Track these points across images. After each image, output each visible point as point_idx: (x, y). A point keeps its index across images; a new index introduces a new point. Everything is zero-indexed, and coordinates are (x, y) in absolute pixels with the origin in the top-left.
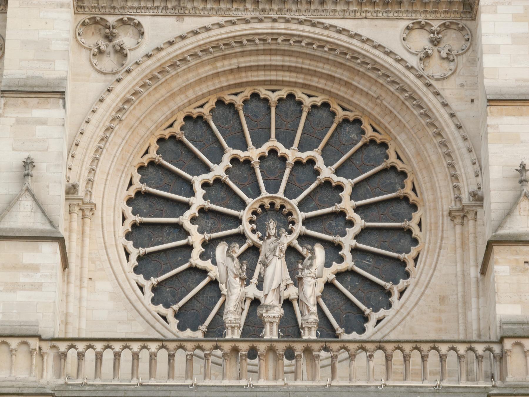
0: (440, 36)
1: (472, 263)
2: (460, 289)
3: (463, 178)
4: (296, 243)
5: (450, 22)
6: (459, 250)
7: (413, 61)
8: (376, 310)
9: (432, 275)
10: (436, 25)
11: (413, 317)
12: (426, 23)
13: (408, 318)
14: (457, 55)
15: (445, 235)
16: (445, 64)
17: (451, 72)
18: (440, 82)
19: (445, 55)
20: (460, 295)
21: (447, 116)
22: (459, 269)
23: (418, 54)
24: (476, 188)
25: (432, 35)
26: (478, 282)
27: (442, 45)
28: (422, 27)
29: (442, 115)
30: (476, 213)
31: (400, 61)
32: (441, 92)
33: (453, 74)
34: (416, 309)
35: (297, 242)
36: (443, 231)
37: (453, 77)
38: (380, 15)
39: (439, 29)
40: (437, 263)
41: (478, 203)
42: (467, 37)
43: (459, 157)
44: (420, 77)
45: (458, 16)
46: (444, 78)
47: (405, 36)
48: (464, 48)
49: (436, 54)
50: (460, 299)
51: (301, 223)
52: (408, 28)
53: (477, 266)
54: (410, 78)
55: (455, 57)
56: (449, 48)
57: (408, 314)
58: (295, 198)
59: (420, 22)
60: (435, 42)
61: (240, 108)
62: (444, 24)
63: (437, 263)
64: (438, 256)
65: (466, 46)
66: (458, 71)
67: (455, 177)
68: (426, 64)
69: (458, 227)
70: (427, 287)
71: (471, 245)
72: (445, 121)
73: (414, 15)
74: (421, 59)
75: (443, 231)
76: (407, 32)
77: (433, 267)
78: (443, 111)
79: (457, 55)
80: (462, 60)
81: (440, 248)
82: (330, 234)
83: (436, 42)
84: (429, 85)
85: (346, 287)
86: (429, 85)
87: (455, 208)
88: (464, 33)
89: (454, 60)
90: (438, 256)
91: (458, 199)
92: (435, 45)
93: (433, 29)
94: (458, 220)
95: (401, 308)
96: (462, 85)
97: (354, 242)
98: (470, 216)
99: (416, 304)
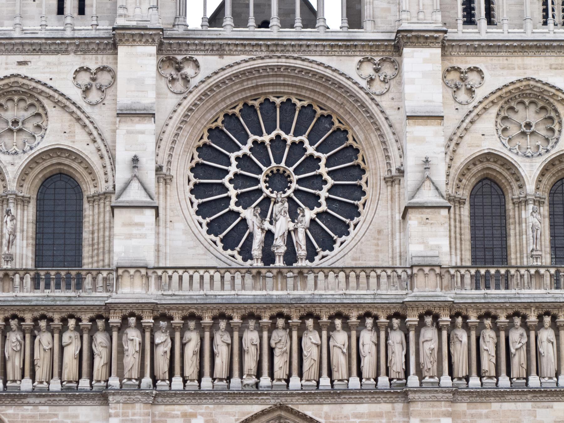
1: (397, 211)
2: (390, 226)
3: (392, 157)
4: (292, 195)
6: (390, 202)
7: (363, 84)
8: (340, 236)
10: (377, 59)
11: (362, 243)
12: (372, 58)
13: (359, 243)
15: (381, 192)
16: (383, 84)
17: (386, 90)
18: (379, 97)
19: (382, 79)
20: (390, 230)
21: (383, 119)
22: (389, 214)
24: (400, 165)
25: (375, 66)
27: (381, 72)
28: (369, 61)
29: (380, 118)
31: (355, 83)
32: (380, 104)
33: (387, 91)
36: (380, 189)
37: (387, 94)
38: (343, 53)
41: (401, 174)
42: (396, 67)
44: (367, 94)
45: (391, 53)
46: (382, 94)
47: (358, 67)
49: (377, 78)
50: (390, 232)
51: (295, 182)
52: (360, 61)
53: (400, 213)
54: (361, 94)
57: (359, 241)
58: (292, 166)
60: (377, 70)
61: (258, 109)
67: (388, 157)
68: (371, 84)
69: (389, 188)
70: (370, 224)
71: (397, 200)
72: (382, 122)
73: (364, 53)
74: (368, 82)
75: (380, 189)
76: (360, 64)
77: (374, 212)
78: (381, 115)
79: (390, 79)
80: (393, 83)
81: (378, 200)
82: (313, 189)
84: (373, 99)
85: (322, 222)
86: (373, 99)
87: (387, 176)
88: (394, 64)
89: (388, 82)
91: (390, 171)
92: (377, 72)
94: (389, 184)
96: (393, 99)
97: (327, 194)
98: (397, 182)
99: (364, 235)
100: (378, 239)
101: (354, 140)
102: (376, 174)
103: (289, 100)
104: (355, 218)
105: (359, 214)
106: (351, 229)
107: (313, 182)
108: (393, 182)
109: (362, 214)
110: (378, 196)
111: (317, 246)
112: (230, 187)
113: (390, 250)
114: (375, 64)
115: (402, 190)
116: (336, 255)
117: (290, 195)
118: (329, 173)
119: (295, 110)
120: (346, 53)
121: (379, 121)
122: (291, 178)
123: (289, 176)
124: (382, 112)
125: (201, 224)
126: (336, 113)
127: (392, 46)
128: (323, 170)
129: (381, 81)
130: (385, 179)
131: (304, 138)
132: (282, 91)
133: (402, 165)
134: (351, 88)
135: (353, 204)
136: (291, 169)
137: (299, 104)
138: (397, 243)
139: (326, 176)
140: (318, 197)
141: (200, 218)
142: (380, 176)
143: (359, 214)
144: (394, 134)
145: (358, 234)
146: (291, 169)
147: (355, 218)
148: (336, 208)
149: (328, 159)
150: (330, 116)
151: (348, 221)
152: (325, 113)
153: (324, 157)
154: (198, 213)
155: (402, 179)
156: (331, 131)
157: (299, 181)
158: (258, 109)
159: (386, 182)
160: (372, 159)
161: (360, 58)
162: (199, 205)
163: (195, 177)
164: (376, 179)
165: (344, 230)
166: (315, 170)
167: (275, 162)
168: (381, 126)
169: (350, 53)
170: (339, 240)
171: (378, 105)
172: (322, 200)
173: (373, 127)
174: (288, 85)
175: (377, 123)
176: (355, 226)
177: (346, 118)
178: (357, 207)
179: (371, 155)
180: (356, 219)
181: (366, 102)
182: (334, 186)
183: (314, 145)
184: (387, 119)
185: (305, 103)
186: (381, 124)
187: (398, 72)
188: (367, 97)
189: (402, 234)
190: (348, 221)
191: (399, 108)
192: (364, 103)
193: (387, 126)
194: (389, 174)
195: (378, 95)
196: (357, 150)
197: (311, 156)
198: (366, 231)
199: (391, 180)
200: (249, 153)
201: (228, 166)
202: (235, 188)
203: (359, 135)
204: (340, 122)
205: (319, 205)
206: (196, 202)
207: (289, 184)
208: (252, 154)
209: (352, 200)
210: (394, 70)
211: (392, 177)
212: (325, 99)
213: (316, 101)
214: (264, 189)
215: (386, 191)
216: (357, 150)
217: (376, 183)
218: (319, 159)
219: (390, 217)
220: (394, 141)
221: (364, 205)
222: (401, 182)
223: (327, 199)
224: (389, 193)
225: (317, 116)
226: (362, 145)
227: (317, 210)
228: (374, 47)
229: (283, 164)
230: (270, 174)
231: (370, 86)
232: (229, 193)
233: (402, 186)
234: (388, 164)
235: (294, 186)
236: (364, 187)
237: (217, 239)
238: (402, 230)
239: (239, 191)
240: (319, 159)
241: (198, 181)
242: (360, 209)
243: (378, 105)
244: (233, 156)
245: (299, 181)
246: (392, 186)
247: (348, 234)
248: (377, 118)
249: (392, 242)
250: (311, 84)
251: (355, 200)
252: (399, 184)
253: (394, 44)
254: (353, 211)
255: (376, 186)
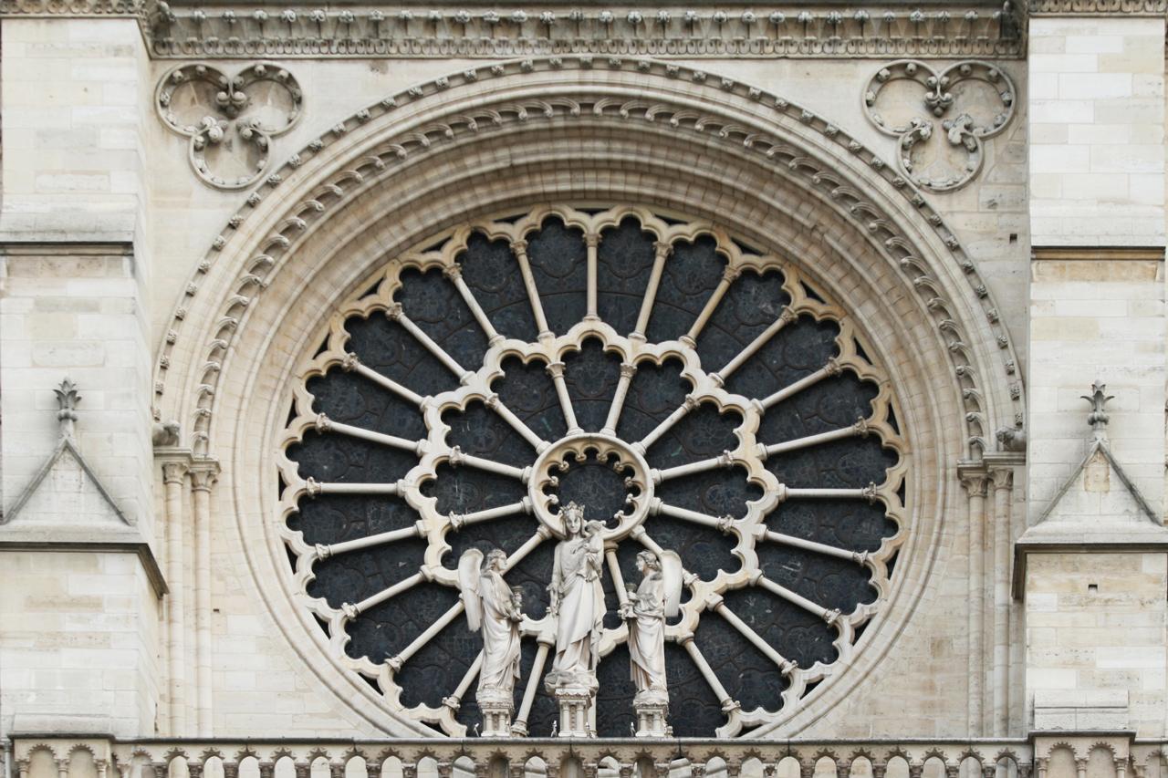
0: (948, 95)
2: (974, 626)
3: (988, 401)
5: (971, 65)
6: (976, 549)
7: (888, 153)
9: (919, 597)
10: (939, 71)
11: (876, 681)
12: (918, 67)
13: (866, 682)
14: (983, 139)
15: (948, 518)
16: (959, 157)
17: (969, 176)
18: (945, 197)
19: (957, 139)
20: (972, 637)
21: (957, 273)
22: (973, 587)
23: (897, 138)
24: (1012, 425)
25: (930, 95)
26: (1008, 612)
27: (952, 116)
28: (910, 76)
29: (947, 271)
30: (1011, 476)
32: (947, 221)
33: (972, 179)
34: (882, 665)
35: (642, 529)
36: (944, 507)
37: (973, 188)
38: (817, 50)
39: (945, 80)
40: (929, 573)
41: (1016, 455)
42: (1006, 98)
43: (980, 359)
44: (901, 187)
45: (989, 50)
46: (953, 190)
47: (870, 96)
48: (998, 122)
49: (939, 136)
52: (877, 78)
55: (979, 142)
56: (967, 121)
57: (867, 674)
59: (906, 65)
60: (938, 110)
62: (958, 68)
63: (929, 573)
64: (933, 559)
65: (1004, 119)
66: (985, 172)
67: (972, 401)
68: (916, 157)
70: (907, 621)
72: (953, 282)
73: (891, 50)
74: (904, 148)
75: (944, 507)
76: (877, 87)
77: (921, 581)
78: (948, 260)
79: (983, 139)
80: (991, 150)
81: (938, 543)
82: (715, 514)
83: (938, 110)
84: (920, 206)
85: (746, 620)
86: (920, 206)
87: (968, 463)
88: (1001, 87)
90: (933, 559)
91: (977, 446)
92: (938, 116)
93: (933, 80)
94: (975, 488)
95: (855, 661)
96: (993, 205)
97: (762, 530)
98: (1000, 480)
99: (885, 654)
100: (933, 669)
101: (860, 352)
102: (933, 461)
103: (631, 222)
104: (859, 605)
105: (871, 595)
106: (843, 642)
107: (714, 492)
108: (987, 481)
109: (882, 595)
110: (936, 529)
111: (723, 695)
112: (427, 505)
113: (974, 703)
114: (933, 89)
115: (1016, 508)
116: (789, 720)
117: (630, 531)
118: (770, 462)
119: (653, 255)
120: (827, 49)
121: (943, 278)
122: (638, 478)
123: (629, 471)
124: (954, 248)
125: (324, 625)
126: (797, 264)
127: (992, 22)
128: (749, 451)
129: (954, 146)
130: (960, 472)
131: (683, 347)
132: (604, 187)
133: (1019, 425)
134: (842, 170)
135: (853, 563)
136: (638, 449)
137: (666, 234)
138: (995, 678)
139: (758, 472)
140: (732, 539)
141: (322, 605)
142: (945, 467)
143: (871, 595)
144: (994, 321)
145: (866, 655)
146: (638, 449)
147: (859, 605)
148: (794, 575)
149: (767, 416)
150: (775, 276)
151: (832, 615)
152: (759, 263)
153: (751, 409)
154: (313, 589)
155: (1017, 470)
156: (778, 325)
157: (663, 489)
158: (521, 250)
159: (965, 485)
160: (920, 412)
161: (879, 67)
162: (318, 565)
163: (303, 474)
164: (935, 478)
165: (817, 642)
166: (721, 453)
167: (580, 425)
168: (949, 299)
169: (841, 50)
170: (801, 677)
171: (937, 224)
172: (745, 549)
173: (923, 303)
174: (625, 168)
175: (936, 287)
176: (859, 630)
177: (832, 276)
178: (866, 571)
179: (917, 400)
180: (861, 611)
181: (897, 218)
182: (786, 504)
183: (717, 370)
184: (969, 271)
185: (689, 231)
186: (950, 289)
187: (1015, 113)
188: (900, 200)
189: (1013, 649)
190: (832, 615)
191: (1013, 238)
192: (889, 218)
193: (969, 295)
194: (976, 456)
195: (939, 192)
196: (871, 388)
197: (709, 406)
198: (891, 645)
199: (983, 476)
200: (489, 396)
201: (416, 439)
202: (443, 510)
203: (876, 333)
204: (810, 294)
205: (735, 564)
206: (308, 554)
207: (629, 498)
208: (502, 400)
209: (850, 549)
210: (1000, 108)
211: (984, 466)
212: (756, 215)
213: (728, 225)
214: (543, 513)
215: (963, 514)
216: (871, 388)
217: (934, 491)
218: (735, 417)
219: (975, 596)
220: (992, 345)
221: (891, 564)
222: (1015, 483)
223: (762, 546)
224: (975, 519)
225: (731, 272)
226: (888, 368)
227: (724, 579)
228: (930, 28)
229: (608, 432)
230: (565, 465)
231: (913, 162)
232: (421, 526)
233: (1017, 493)
234: (974, 423)
235: (647, 502)
236: (893, 507)
237: (382, 672)
238: (1013, 637)
239: (456, 520)
240: (735, 417)
241: (312, 486)
242: (878, 576)
243: (937, 224)
244: (433, 406)
245: (663, 489)
246: (984, 496)
247: (833, 655)
248: (936, 267)
249: (982, 677)
250: (703, 162)
251: (858, 548)
252: (1009, 488)
253: (1002, 17)
254: (854, 585)
255: (933, 501)
